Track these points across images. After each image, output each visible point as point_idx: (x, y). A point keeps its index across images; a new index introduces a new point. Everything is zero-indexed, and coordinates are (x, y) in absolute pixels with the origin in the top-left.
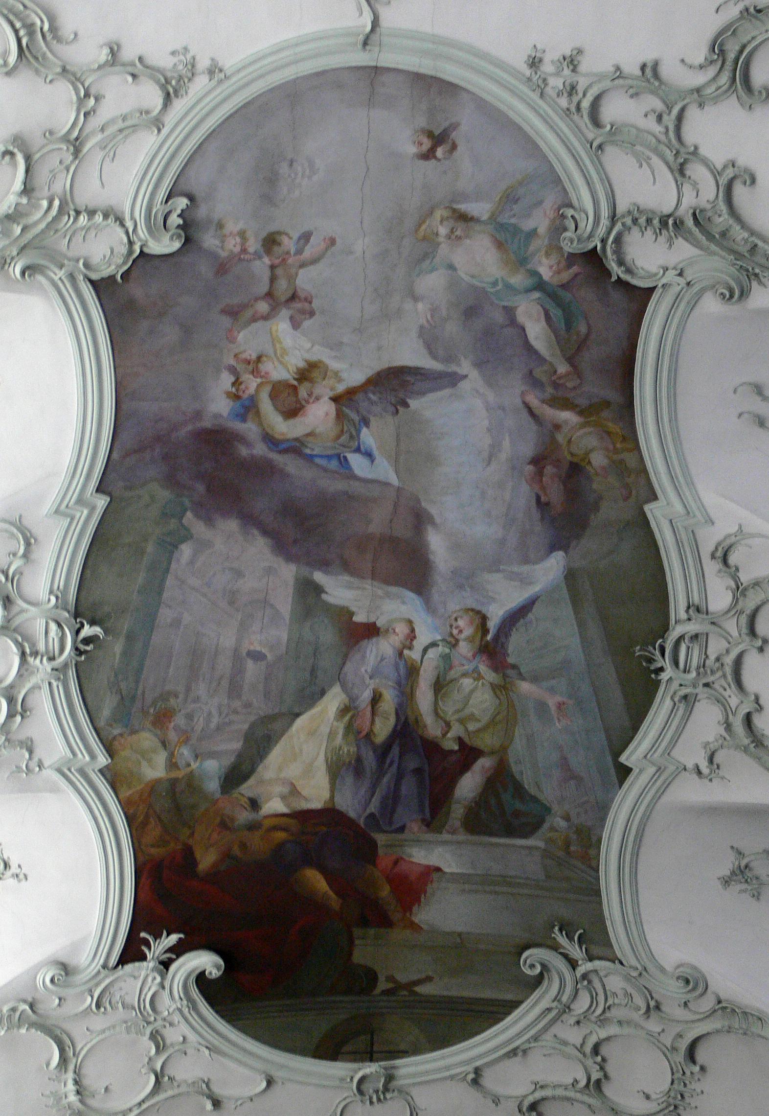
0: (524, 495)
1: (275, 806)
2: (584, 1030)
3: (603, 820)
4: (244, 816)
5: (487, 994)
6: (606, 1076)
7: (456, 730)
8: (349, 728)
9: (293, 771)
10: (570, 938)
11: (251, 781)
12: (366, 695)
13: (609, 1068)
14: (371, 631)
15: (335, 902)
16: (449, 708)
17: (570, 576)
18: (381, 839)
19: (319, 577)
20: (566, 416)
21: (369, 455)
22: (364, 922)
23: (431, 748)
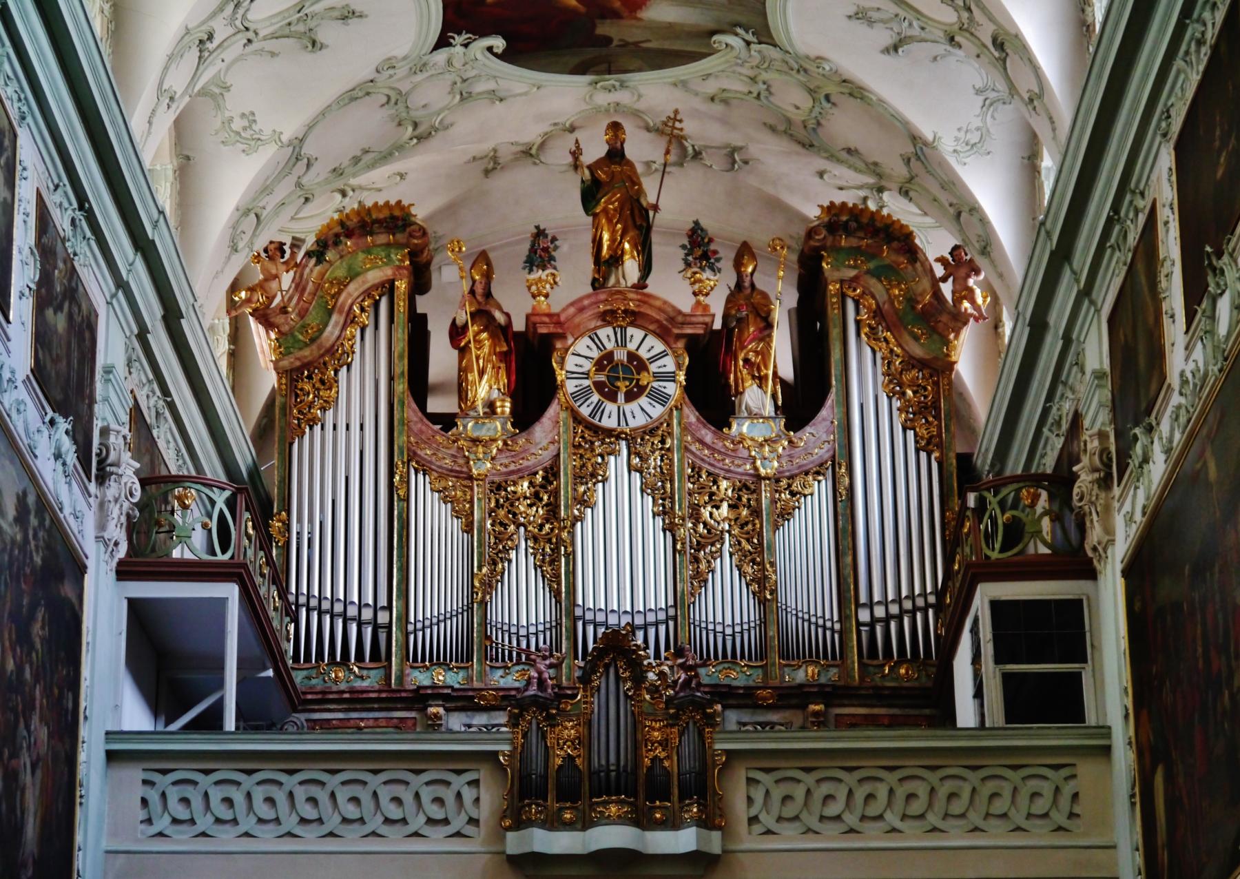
2: (756, 71)
5: (689, 48)
6: (771, 93)
10: (747, 32)
13: (773, 90)
22: (603, 17)
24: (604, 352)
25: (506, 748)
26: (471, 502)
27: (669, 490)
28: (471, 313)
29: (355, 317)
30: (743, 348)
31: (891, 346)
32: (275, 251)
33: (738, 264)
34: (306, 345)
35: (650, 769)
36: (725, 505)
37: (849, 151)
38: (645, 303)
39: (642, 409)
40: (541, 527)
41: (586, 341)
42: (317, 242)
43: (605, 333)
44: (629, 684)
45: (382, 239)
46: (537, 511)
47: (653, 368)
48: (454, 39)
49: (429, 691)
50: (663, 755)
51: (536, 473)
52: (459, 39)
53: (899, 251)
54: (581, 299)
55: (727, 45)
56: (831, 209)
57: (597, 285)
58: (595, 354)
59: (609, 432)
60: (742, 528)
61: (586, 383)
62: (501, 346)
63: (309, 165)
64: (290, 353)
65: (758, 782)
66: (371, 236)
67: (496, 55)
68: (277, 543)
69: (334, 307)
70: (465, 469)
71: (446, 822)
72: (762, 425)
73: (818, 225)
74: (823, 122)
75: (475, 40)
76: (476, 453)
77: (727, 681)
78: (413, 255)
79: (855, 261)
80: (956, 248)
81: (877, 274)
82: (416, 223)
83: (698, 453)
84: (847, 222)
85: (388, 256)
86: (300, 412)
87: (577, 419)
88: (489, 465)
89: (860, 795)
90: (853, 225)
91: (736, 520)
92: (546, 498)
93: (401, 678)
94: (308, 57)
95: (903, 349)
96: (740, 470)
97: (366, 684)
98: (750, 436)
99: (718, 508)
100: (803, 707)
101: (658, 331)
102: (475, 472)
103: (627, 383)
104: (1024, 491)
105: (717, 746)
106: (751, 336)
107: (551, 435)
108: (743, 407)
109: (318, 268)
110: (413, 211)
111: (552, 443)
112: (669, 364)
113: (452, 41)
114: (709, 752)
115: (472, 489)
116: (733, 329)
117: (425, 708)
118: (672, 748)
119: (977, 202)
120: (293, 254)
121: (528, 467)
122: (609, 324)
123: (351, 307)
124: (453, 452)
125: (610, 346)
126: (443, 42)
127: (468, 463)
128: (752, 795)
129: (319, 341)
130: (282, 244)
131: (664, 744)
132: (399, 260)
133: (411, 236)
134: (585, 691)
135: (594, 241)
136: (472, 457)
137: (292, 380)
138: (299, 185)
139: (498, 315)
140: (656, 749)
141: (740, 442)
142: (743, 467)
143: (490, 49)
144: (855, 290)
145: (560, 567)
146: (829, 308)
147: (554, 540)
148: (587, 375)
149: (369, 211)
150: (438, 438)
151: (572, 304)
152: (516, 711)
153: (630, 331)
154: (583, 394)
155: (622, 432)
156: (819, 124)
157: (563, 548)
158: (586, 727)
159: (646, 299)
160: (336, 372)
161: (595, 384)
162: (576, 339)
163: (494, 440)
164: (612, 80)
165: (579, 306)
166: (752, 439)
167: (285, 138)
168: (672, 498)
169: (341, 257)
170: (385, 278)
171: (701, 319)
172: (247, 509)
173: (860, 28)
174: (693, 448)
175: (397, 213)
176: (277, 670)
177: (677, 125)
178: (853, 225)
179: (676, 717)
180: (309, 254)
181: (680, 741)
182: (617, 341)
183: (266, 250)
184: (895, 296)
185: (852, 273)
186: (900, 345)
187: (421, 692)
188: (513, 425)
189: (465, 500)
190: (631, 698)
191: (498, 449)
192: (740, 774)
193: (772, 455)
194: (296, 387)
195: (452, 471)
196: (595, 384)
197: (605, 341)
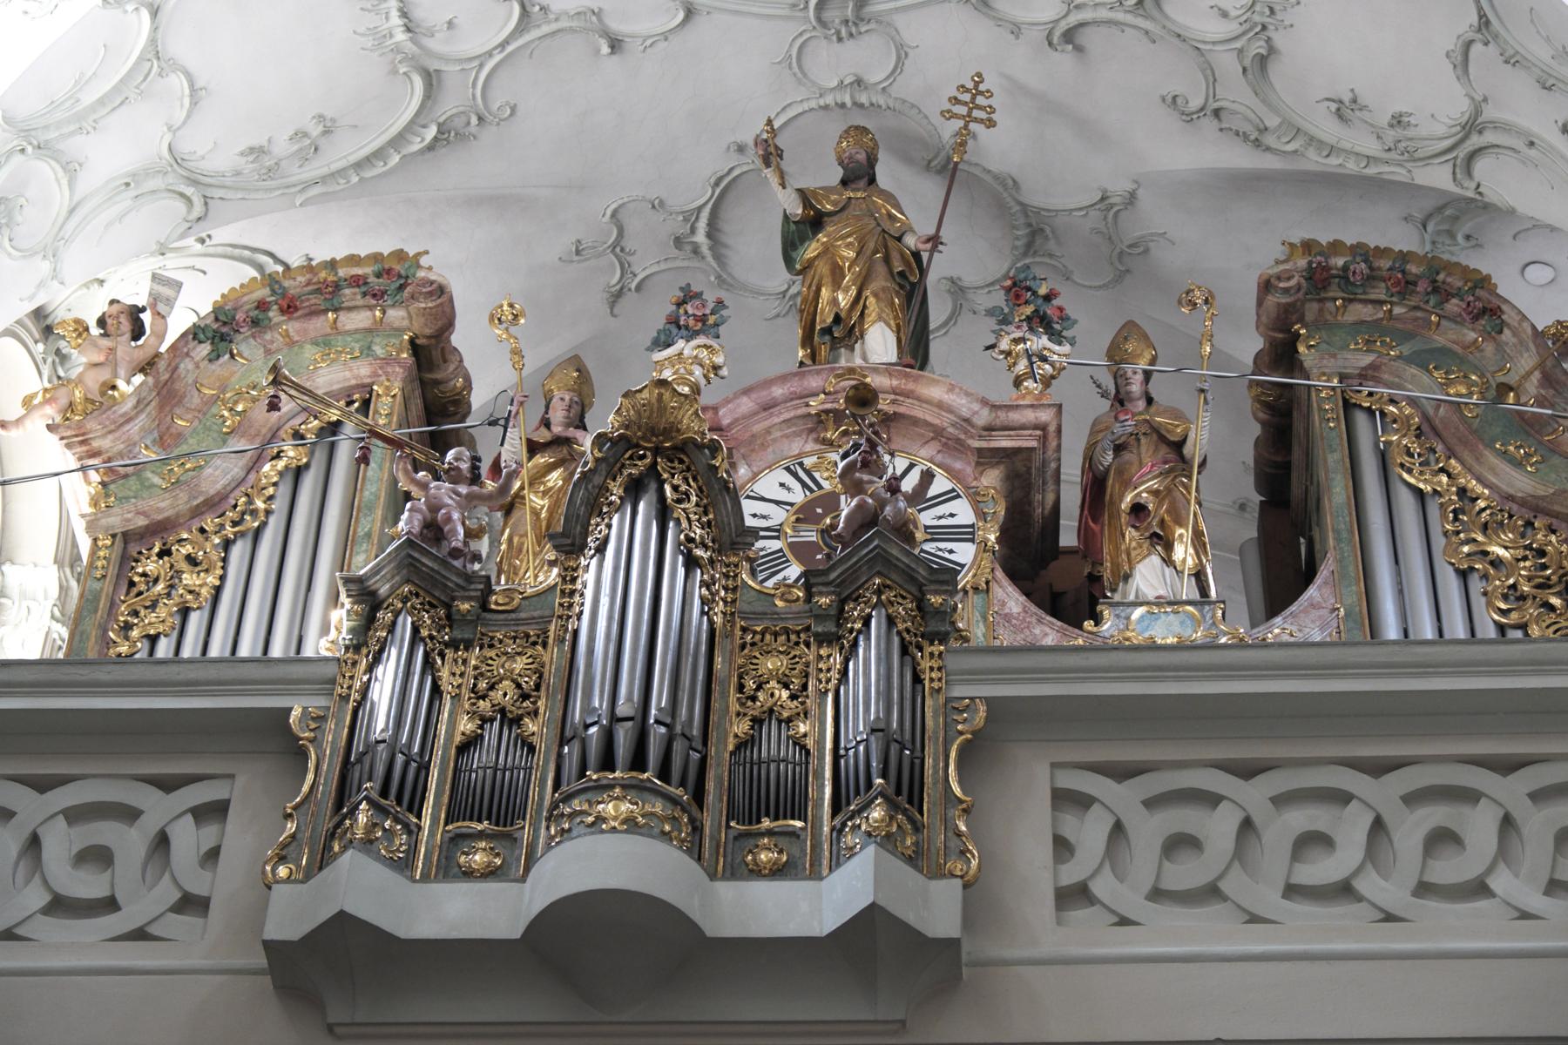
58: (798, 496)
65: (1083, 802)
66: (336, 310)
71: (110, 904)
74: (1279, 39)
81: (1422, 360)
84: (1345, 268)
89: (1409, 831)
112: (962, 512)
128: (1068, 832)
156: (1272, 50)
160: (227, 544)
161: (792, 546)
170: (353, 382)
171: (1029, 416)
177: (980, 100)
180: (195, 334)
185: (1368, 359)
196: (792, 546)
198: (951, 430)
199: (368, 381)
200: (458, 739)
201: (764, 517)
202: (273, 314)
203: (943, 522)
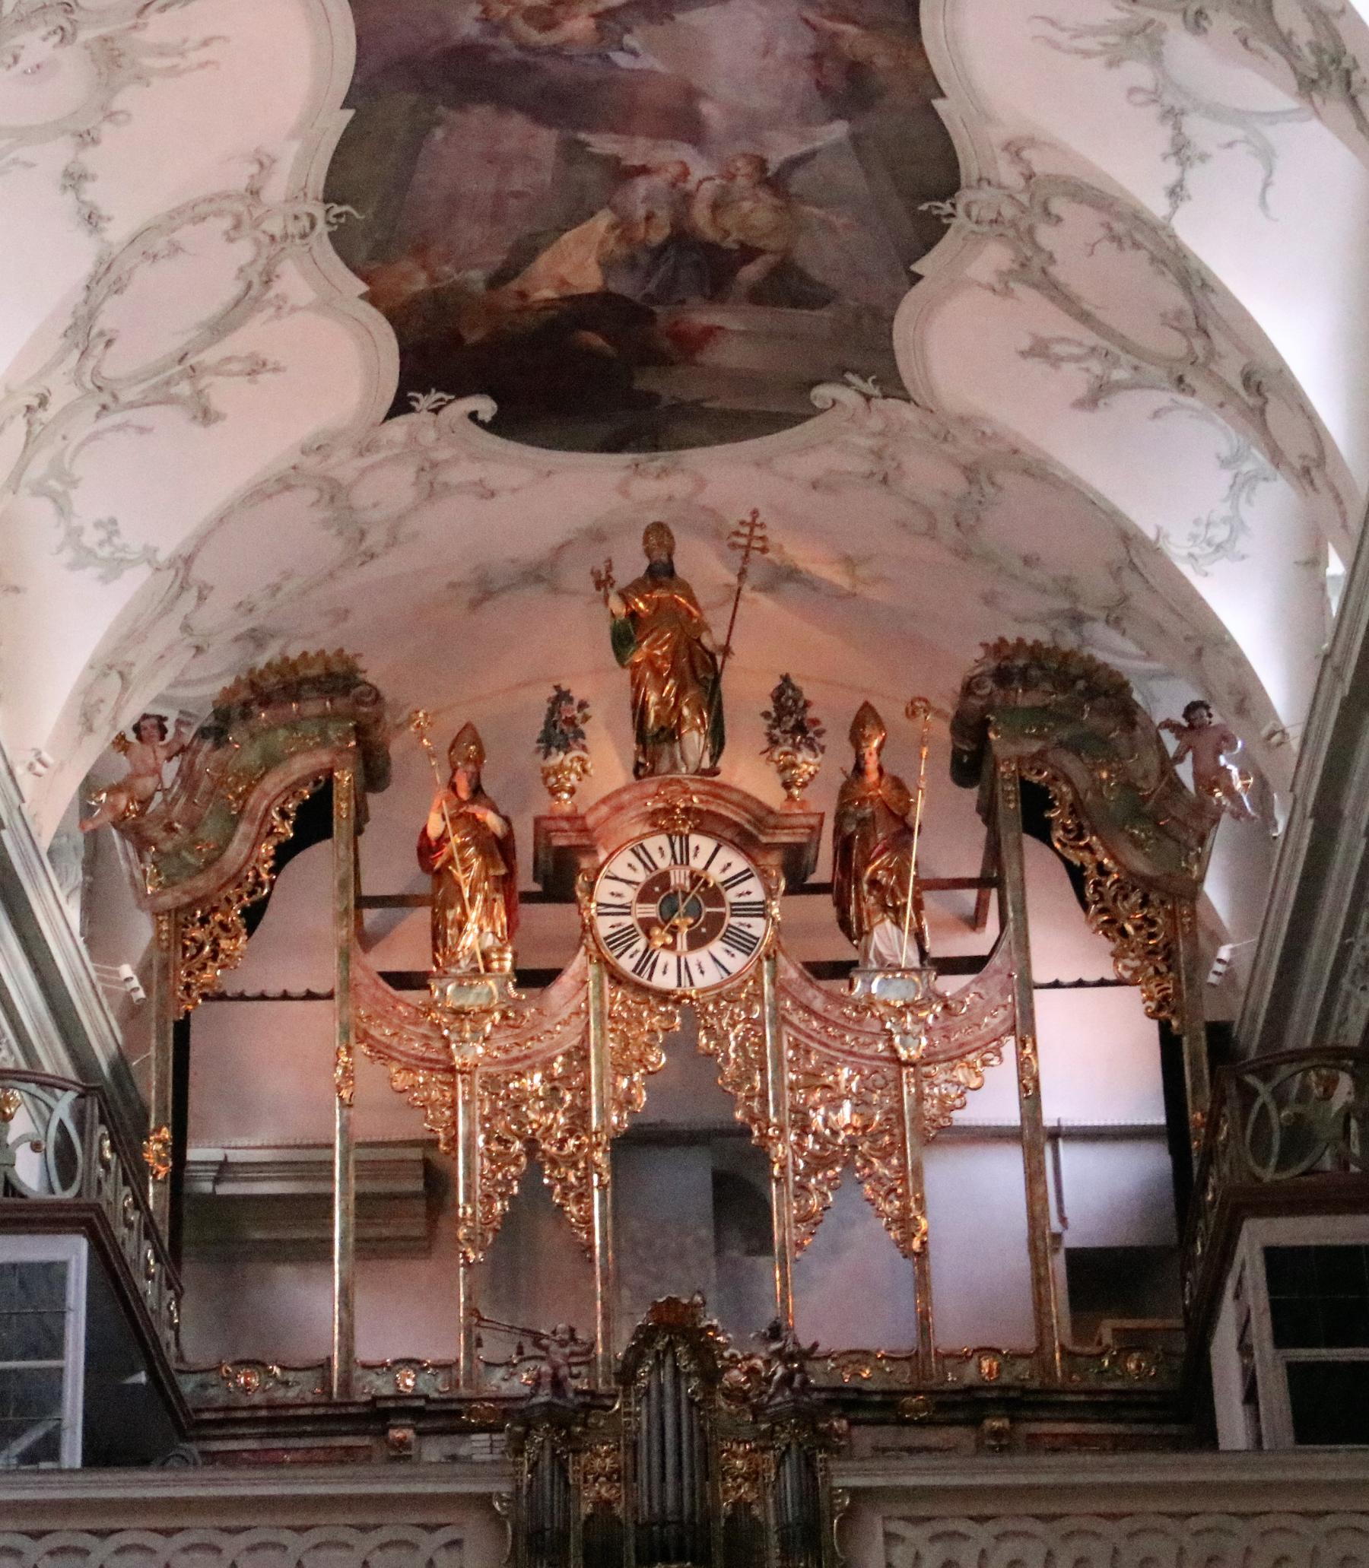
0: (803, 80)
1: (548, 293)
3: (895, 307)
4: (513, 303)
7: (735, 235)
8: (619, 239)
9: (564, 270)
11: (517, 280)
12: (641, 212)
14: (643, 170)
15: (610, 351)
16: (729, 221)
17: (855, 139)
18: (657, 309)
19: (582, 136)
20: (850, 29)
21: (633, 53)
23: (711, 249)
24: (655, 873)
25: (505, 1488)
26: (453, 1106)
27: (758, 1085)
28: (452, 819)
29: (273, 827)
30: (868, 863)
31: (1099, 857)
32: (150, 728)
33: (857, 738)
34: (200, 871)
35: (730, 1520)
36: (847, 1106)
37: (1027, 561)
38: (716, 796)
39: (715, 960)
40: (563, 1141)
41: (627, 856)
42: (216, 713)
43: (656, 844)
44: (695, 1383)
45: (313, 708)
46: (555, 1119)
47: (731, 896)
48: (417, 400)
49: (391, 1404)
50: (753, 1496)
51: (553, 1059)
52: (425, 402)
53: (1103, 713)
54: (618, 792)
55: (834, 402)
56: (998, 648)
57: (641, 772)
58: (641, 876)
59: (664, 996)
60: (874, 1142)
61: (628, 921)
62: (495, 866)
63: (201, 598)
64: (174, 884)
65: (901, 1539)
66: (297, 701)
67: (482, 424)
68: (155, 1176)
69: (241, 812)
70: (442, 1057)
72: (899, 983)
73: (981, 675)
75: (450, 401)
76: (460, 1032)
77: (855, 1384)
78: (360, 731)
79: (1040, 728)
80: (1191, 709)
81: (1074, 747)
82: (365, 683)
83: (802, 1026)
84: (1026, 668)
85: (323, 733)
86: (190, 974)
87: (618, 979)
88: (480, 1050)
90: (1034, 673)
91: (865, 1127)
92: (568, 1097)
93: (346, 1384)
94: (197, 430)
95: (1117, 862)
96: (868, 1052)
97: (292, 1394)
98: (883, 998)
99: (837, 1108)
100: (975, 1422)
101: (737, 840)
102: (458, 1061)
103: (691, 921)
104: (1312, 1074)
105: (837, 1482)
106: (880, 847)
107: (575, 1002)
108: (871, 955)
109: (217, 754)
110: (362, 664)
111: (577, 1014)
112: (754, 890)
113: (414, 404)
114: (823, 1495)
115: (453, 1086)
116: (851, 836)
117: (385, 1432)
118: (766, 1486)
119: (1225, 631)
120: (178, 733)
121: (539, 1052)
122: (662, 830)
123: (267, 811)
124: (423, 1030)
125: (663, 864)
126: (401, 406)
127: (448, 1046)
129: (217, 866)
130: (161, 719)
131: (753, 1476)
132: (339, 738)
133: (359, 702)
134: (626, 1396)
135: (634, 705)
136: (454, 1037)
137: (177, 925)
138: (186, 628)
139: (492, 821)
140: (739, 1487)
141: (866, 1009)
142: (873, 1047)
143: (473, 416)
144: (1040, 772)
145: (592, 1207)
146: (1000, 799)
147: (582, 1165)
148: (625, 910)
149: (294, 666)
150: (401, 1008)
151: (604, 801)
152: (519, 1429)
153: (695, 840)
154: (622, 939)
155: (684, 996)
157: (595, 1177)
158: (630, 1454)
159: (719, 791)
161: (641, 921)
162: (611, 855)
163: (488, 1012)
164: (662, 459)
165: (614, 802)
166: (886, 1004)
167: (162, 557)
168: (763, 1095)
169: (253, 736)
170: (318, 768)
171: (803, 820)
172: (102, 1121)
173: (1036, 368)
174: (794, 1018)
175: (337, 668)
176: (152, 1373)
178: (1034, 673)
179: (771, 1434)
180: (203, 733)
181: (777, 1474)
182: (674, 856)
183: (137, 729)
184: (1101, 779)
185: (1035, 747)
186: (1113, 857)
187: (381, 1405)
188: (517, 986)
189: (443, 1105)
190: (699, 1406)
191: (494, 1025)
192: (875, 1525)
193: (917, 1028)
194: (183, 935)
195: (423, 1059)
197: (656, 857)
198: (747, 826)
199: (328, 766)
200: (583, 1518)
201: (619, 895)
202: (254, 708)
203: (743, 899)
